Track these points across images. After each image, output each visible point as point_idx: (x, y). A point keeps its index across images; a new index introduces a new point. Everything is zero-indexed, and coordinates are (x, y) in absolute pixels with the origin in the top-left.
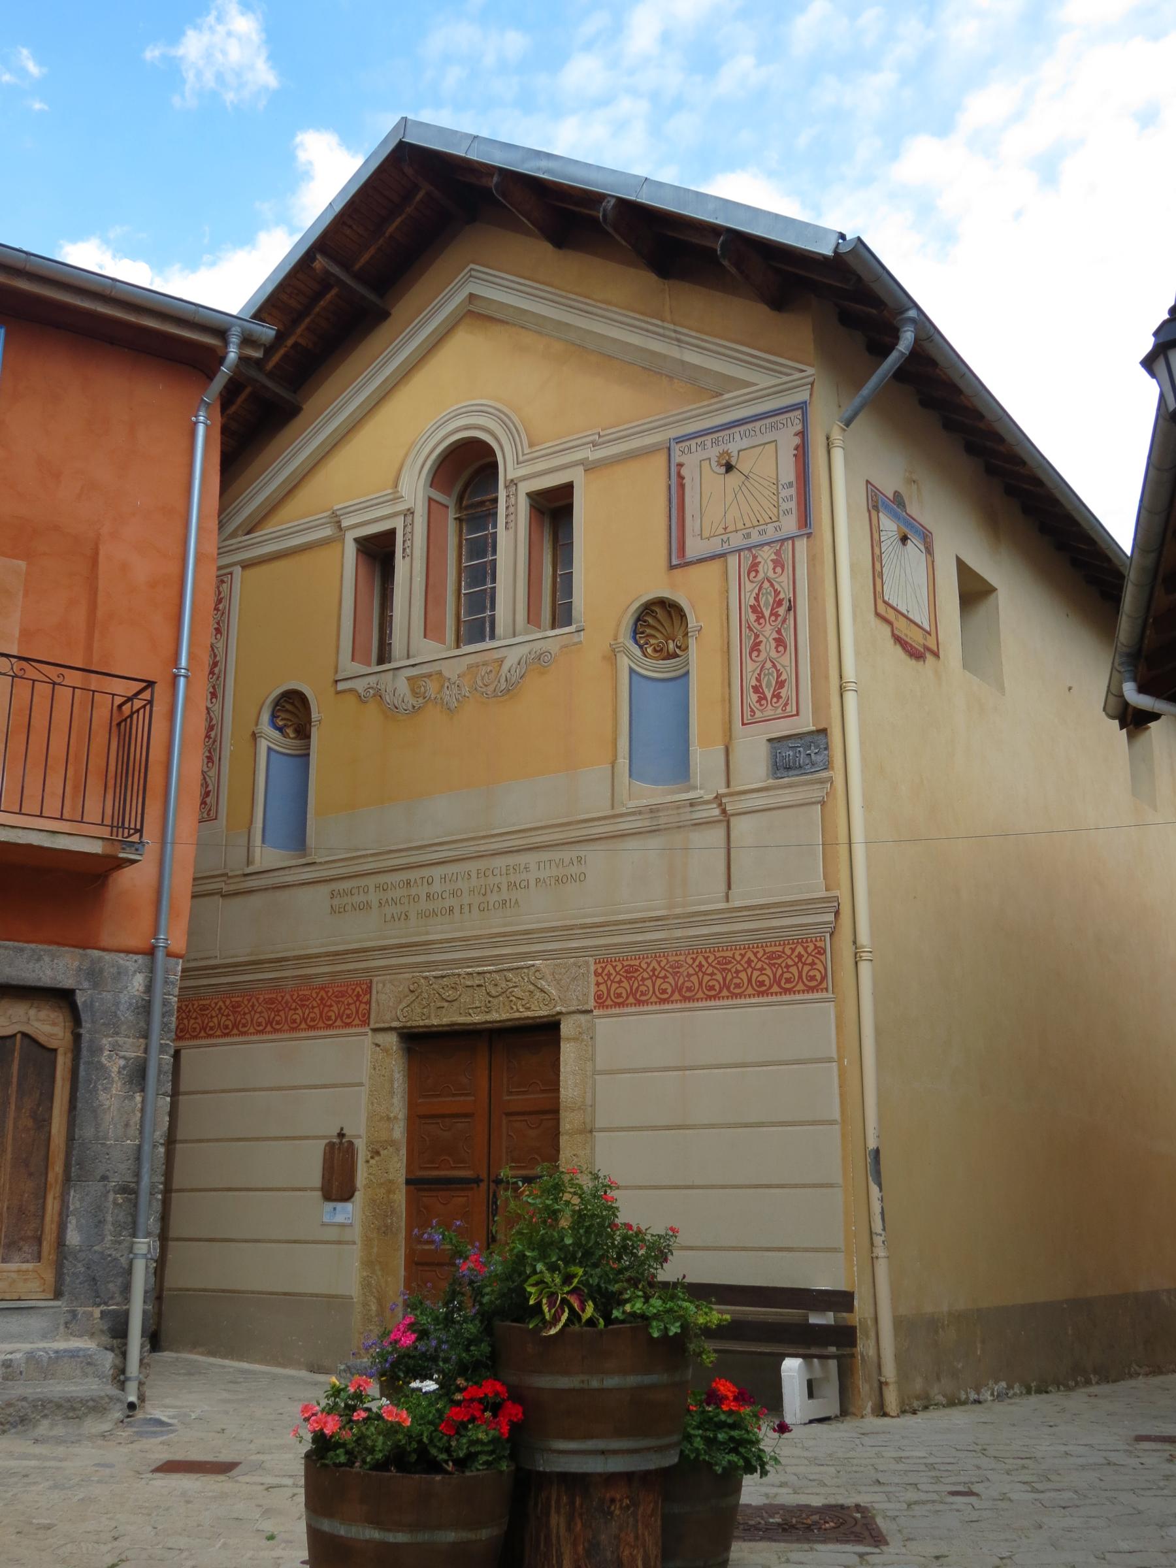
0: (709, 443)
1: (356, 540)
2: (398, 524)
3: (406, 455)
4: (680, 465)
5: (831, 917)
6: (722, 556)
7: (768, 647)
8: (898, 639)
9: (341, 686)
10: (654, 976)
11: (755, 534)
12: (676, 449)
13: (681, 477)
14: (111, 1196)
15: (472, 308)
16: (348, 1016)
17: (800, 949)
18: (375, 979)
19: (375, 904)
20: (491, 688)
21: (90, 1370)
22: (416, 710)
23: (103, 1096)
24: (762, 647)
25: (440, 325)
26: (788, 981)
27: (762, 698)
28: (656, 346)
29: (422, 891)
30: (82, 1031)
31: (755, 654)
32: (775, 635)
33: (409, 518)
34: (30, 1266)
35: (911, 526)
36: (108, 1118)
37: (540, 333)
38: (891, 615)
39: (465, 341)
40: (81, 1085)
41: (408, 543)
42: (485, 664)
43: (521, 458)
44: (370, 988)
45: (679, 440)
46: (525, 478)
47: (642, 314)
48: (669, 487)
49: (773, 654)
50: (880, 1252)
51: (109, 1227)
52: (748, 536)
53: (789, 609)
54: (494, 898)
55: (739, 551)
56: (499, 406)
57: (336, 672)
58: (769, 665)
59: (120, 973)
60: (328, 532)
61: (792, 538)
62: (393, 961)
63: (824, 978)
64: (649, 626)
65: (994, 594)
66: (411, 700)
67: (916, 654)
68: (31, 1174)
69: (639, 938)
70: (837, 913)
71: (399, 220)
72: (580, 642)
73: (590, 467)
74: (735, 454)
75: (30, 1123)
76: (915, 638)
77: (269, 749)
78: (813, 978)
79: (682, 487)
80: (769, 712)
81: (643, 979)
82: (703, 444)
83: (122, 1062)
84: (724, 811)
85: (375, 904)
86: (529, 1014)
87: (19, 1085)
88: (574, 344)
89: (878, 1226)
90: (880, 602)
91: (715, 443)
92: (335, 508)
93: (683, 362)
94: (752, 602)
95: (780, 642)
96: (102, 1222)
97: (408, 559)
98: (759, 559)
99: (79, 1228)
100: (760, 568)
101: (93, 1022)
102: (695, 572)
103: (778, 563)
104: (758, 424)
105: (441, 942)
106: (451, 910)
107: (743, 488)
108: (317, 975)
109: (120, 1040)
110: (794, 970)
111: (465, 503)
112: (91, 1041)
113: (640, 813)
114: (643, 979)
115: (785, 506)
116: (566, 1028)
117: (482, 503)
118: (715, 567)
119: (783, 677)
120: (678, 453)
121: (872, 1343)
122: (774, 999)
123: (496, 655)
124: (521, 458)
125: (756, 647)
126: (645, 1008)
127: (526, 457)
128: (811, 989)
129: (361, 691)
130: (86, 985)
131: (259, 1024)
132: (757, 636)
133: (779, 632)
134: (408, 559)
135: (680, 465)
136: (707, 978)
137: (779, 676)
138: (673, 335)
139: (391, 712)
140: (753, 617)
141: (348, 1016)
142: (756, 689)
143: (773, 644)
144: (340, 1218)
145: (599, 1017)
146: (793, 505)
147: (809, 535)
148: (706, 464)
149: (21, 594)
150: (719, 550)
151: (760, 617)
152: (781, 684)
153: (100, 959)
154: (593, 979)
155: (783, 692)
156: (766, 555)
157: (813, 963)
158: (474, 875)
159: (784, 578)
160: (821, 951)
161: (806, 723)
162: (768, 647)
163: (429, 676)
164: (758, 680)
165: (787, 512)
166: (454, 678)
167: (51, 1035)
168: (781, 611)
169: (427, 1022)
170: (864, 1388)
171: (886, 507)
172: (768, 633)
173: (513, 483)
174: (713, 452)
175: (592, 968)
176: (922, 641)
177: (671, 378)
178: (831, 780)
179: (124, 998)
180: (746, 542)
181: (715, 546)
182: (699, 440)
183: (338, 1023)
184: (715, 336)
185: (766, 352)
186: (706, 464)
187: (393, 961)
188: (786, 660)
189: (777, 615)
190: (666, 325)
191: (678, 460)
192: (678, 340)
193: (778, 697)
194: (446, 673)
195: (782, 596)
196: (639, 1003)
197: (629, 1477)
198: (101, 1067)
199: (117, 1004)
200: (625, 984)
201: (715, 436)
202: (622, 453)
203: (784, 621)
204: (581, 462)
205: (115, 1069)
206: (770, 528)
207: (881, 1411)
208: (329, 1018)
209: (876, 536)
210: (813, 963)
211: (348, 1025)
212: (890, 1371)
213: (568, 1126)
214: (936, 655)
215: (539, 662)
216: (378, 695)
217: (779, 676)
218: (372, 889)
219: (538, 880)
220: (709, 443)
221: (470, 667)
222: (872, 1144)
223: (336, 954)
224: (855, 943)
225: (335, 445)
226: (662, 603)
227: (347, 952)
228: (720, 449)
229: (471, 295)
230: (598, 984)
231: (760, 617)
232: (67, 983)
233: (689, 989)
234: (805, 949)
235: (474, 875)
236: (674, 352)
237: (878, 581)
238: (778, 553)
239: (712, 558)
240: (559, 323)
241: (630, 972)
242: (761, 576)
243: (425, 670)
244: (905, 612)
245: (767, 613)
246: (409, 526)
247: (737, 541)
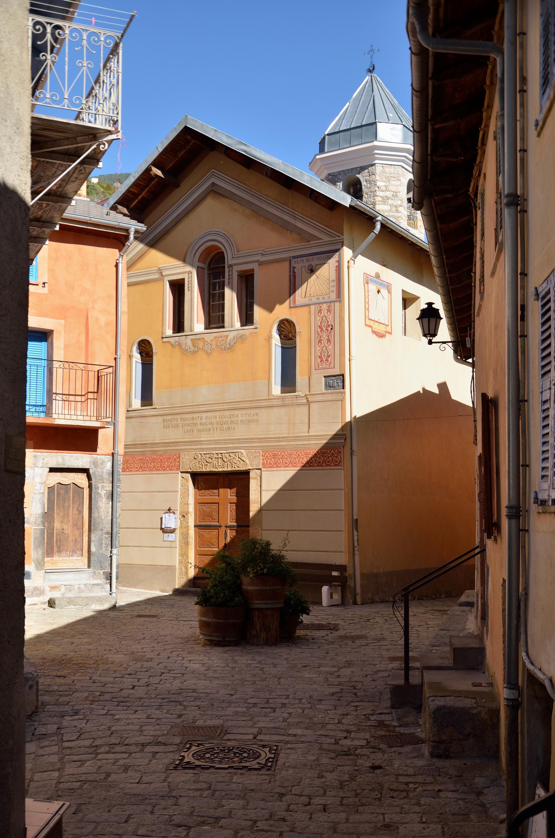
0: (305, 260)
1: (169, 281)
2: (186, 276)
3: (188, 248)
4: (294, 268)
5: (343, 441)
6: (309, 305)
7: (324, 342)
8: (374, 332)
9: (165, 340)
10: (283, 457)
11: (321, 298)
12: (293, 261)
13: (294, 273)
14: (104, 535)
15: (213, 189)
16: (171, 467)
17: (332, 451)
18: (181, 453)
19: (180, 425)
20: (223, 347)
21: (103, 590)
22: (194, 352)
23: (100, 503)
24: (322, 342)
25: (201, 193)
26: (328, 462)
27: (322, 361)
28: (286, 218)
29: (199, 422)
30: (92, 482)
31: (320, 344)
32: (327, 338)
33: (190, 275)
34: (80, 558)
35: (381, 284)
36: (102, 510)
37: (241, 205)
38: (371, 323)
39: (210, 203)
40: (93, 500)
41: (190, 285)
42: (221, 337)
43: (234, 256)
44: (180, 456)
45: (294, 257)
46: (235, 265)
47: (280, 203)
48: (290, 276)
49: (326, 345)
50: (356, 552)
51: (104, 545)
52: (318, 299)
53: (332, 329)
54: (225, 426)
55: (315, 304)
56: (225, 233)
57: (162, 334)
58: (324, 348)
59: (103, 462)
60: (157, 276)
61: (334, 302)
62: (188, 447)
63: (340, 461)
64: (282, 328)
65: (419, 300)
66: (192, 348)
67: (381, 336)
68: (78, 529)
69: (278, 444)
70: (345, 440)
71: (184, 152)
72: (257, 332)
73: (261, 263)
74: (314, 266)
75: (77, 512)
76: (381, 329)
77: (136, 361)
78: (337, 461)
79: (295, 276)
80: (324, 366)
81: (279, 459)
82: (303, 260)
83: (105, 492)
84: (308, 401)
85: (180, 425)
86: (239, 469)
87: (73, 500)
88: (254, 211)
89: (356, 544)
90: (367, 320)
91: (307, 260)
92: (160, 266)
93: (296, 226)
94: (319, 324)
95: (329, 340)
96: (101, 544)
97: (190, 292)
98: (322, 308)
99: (95, 545)
100: (322, 312)
101: (96, 479)
102: (299, 310)
103: (329, 310)
104: (323, 255)
105: (206, 441)
106: (210, 430)
107: (316, 283)
108: (159, 451)
109: (104, 484)
110: (330, 458)
111: (211, 267)
112: (95, 485)
113: (278, 399)
114: (279, 459)
115: (331, 289)
116: (252, 474)
117: (218, 268)
118: (306, 309)
119: (329, 354)
120: (293, 263)
121: (353, 582)
122: (324, 468)
123: (225, 334)
124: (234, 256)
125: (320, 341)
126: (280, 469)
127: (236, 256)
128: (336, 465)
129: (172, 342)
130: (93, 467)
131: (137, 468)
132: (321, 337)
133: (328, 337)
134: (190, 292)
135: (294, 268)
136: (301, 459)
137: (328, 353)
138: (292, 214)
139: (185, 352)
140: (319, 330)
141: (171, 467)
142: (320, 357)
143: (326, 341)
144: (170, 539)
145: (264, 471)
146: (334, 289)
147: (340, 301)
148: (303, 268)
149: (63, 332)
150: (308, 303)
151: (322, 330)
152: (329, 356)
153: (97, 457)
154: (261, 458)
155: (329, 359)
156: (325, 307)
157: (337, 456)
158: (218, 417)
159: (330, 317)
160: (340, 452)
161: (337, 372)
162: (324, 342)
163: (199, 339)
164: (321, 354)
165: (332, 291)
166: (209, 341)
167: (82, 483)
168: (329, 329)
169: (201, 470)
170: (349, 596)
171: (371, 280)
172: (325, 336)
173: (230, 266)
174: (307, 264)
175: (261, 454)
176: (384, 330)
177: (291, 232)
178: (345, 393)
179: (105, 470)
180: (317, 301)
181: (306, 301)
182: (301, 259)
183: (168, 469)
184: (307, 217)
185: (326, 226)
186: (303, 268)
187: (188, 447)
188: (330, 347)
189: (328, 330)
190: (289, 209)
191: (294, 265)
192: (294, 217)
193: (327, 361)
194: (206, 339)
195: (330, 323)
196: (278, 467)
197: (272, 609)
198: (99, 494)
199: (103, 473)
200: (273, 460)
201: (307, 258)
202: (272, 260)
203: (330, 333)
204: (257, 261)
205: (103, 494)
206: (326, 297)
207: (355, 603)
208: (164, 467)
209: (367, 294)
210: (337, 456)
211: (171, 470)
212: (358, 590)
213: (253, 509)
214: (391, 333)
215: (242, 338)
216: (180, 345)
217: (328, 353)
218: (179, 420)
219: (241, 421)
220: (305, 260)
221: (215, 337)
222: (355, 517)
223: (166, 443)
224: (351, 449)
225: (159, 239)
226: (287, 320)
227: (169, 443)
228: (309, 263)
229: (213, 183)
230: (263, 459)
231: (322, 330)
232: (86, 466)
233: (295, 463)
234: (335, 451)
235: (218, 417)
236: (292, 221)
237: (367, 312)
238: (329, 307)
239: (306, 305)
240: (248, 201)
241: (275, 456)
242: (323, 315)
243: (198, 337)
244: (377, 320)
245: (324, 329)
246: (190, 278)
247: (314, 300)
